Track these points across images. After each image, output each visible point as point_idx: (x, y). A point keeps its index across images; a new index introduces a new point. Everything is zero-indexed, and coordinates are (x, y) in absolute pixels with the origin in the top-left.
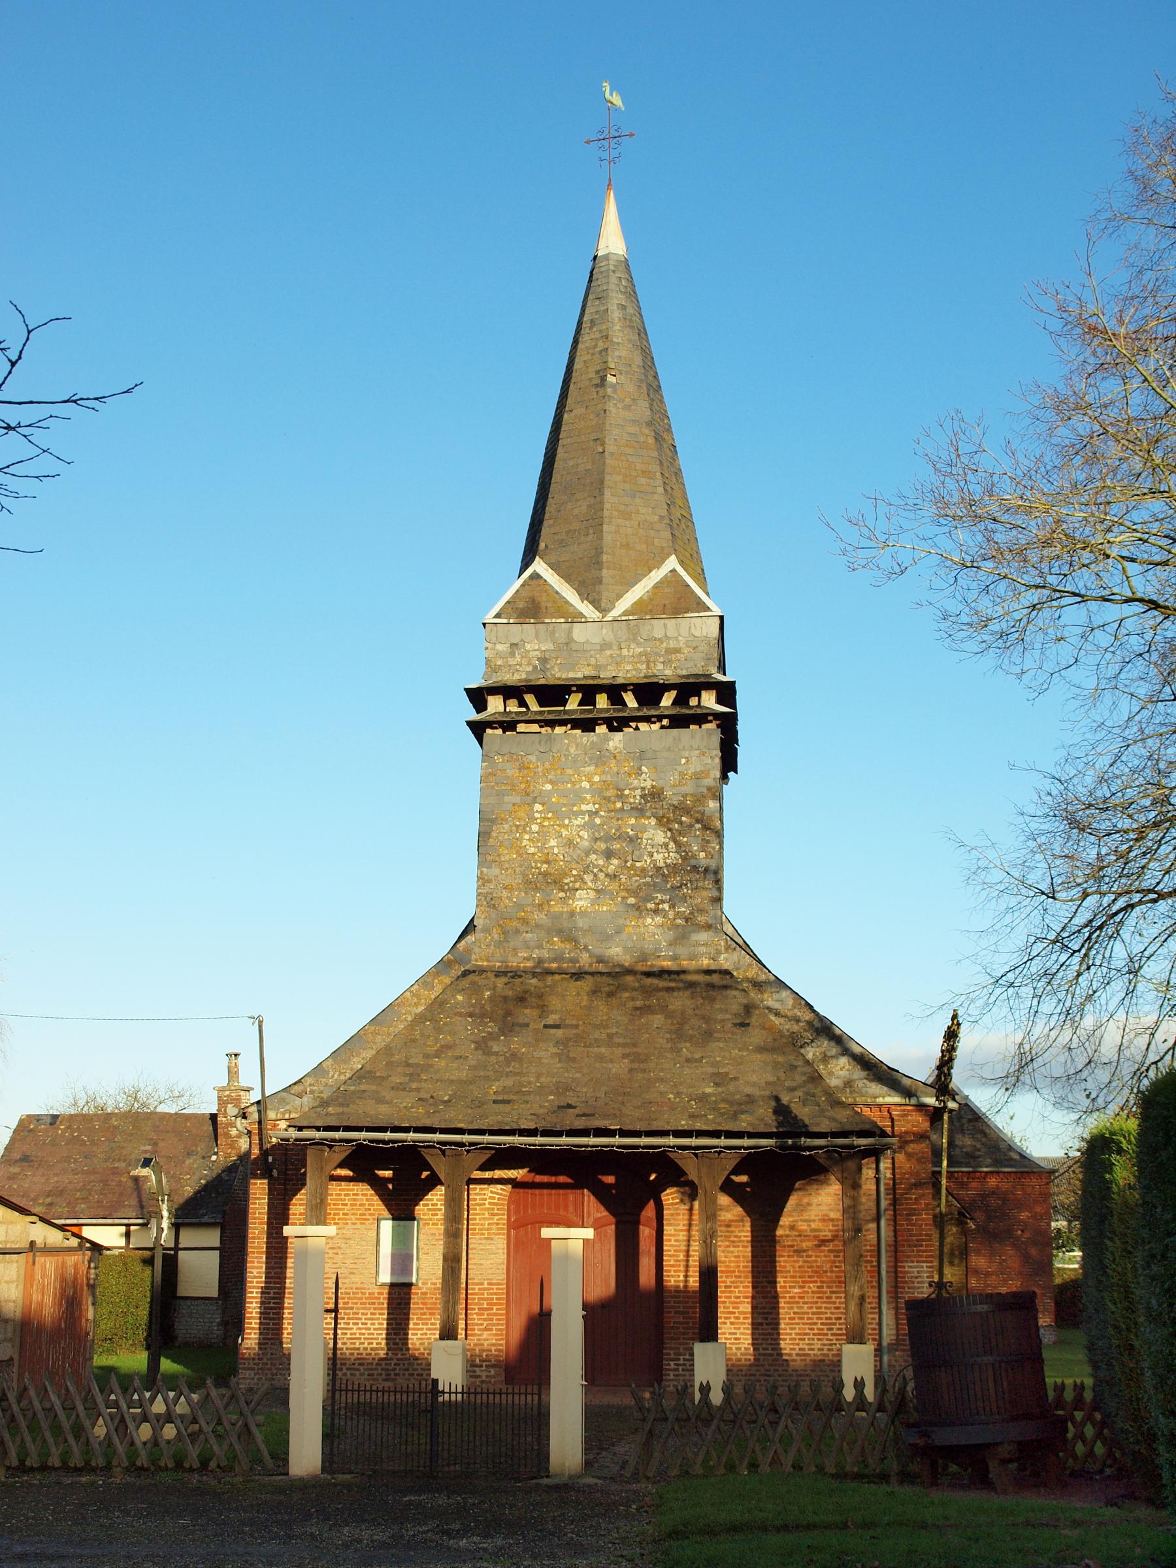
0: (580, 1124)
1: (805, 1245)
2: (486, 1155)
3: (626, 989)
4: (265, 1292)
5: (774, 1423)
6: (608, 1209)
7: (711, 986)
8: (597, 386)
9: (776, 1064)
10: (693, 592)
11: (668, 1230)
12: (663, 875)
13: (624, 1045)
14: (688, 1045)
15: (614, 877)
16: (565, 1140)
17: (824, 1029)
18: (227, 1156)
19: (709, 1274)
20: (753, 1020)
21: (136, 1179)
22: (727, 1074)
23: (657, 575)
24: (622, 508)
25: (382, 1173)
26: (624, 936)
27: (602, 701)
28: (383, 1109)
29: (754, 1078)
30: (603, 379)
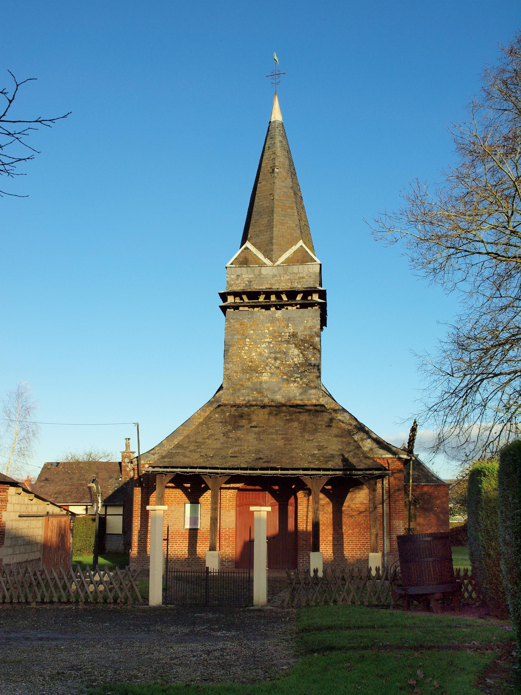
0: (265, 465)
1: (354, 513)
2: (227, 478)
3: (283, 413)
4: (140, 532)
5: (343, 585)
6: (275, 499)
7: (316, 411)
8: (271, 173)
9: (342, 441)
10: (309, 254)
11: (299, 507)
12: (298, 367)
13: (282, 434)
14: (308, 434)
15: (278, 368)
16: (258, 472)
17: (361, 428)
19: (316, 525)
20: (333, 424)
21: (90, 488)
22: (323, 446)
23: (295, 248)
24: (281, 221)
25: (186, 485)
26: (282, 391)
27: (273, 298)
28: (186, 459)
29: (334, 447)
30: (273, 170)
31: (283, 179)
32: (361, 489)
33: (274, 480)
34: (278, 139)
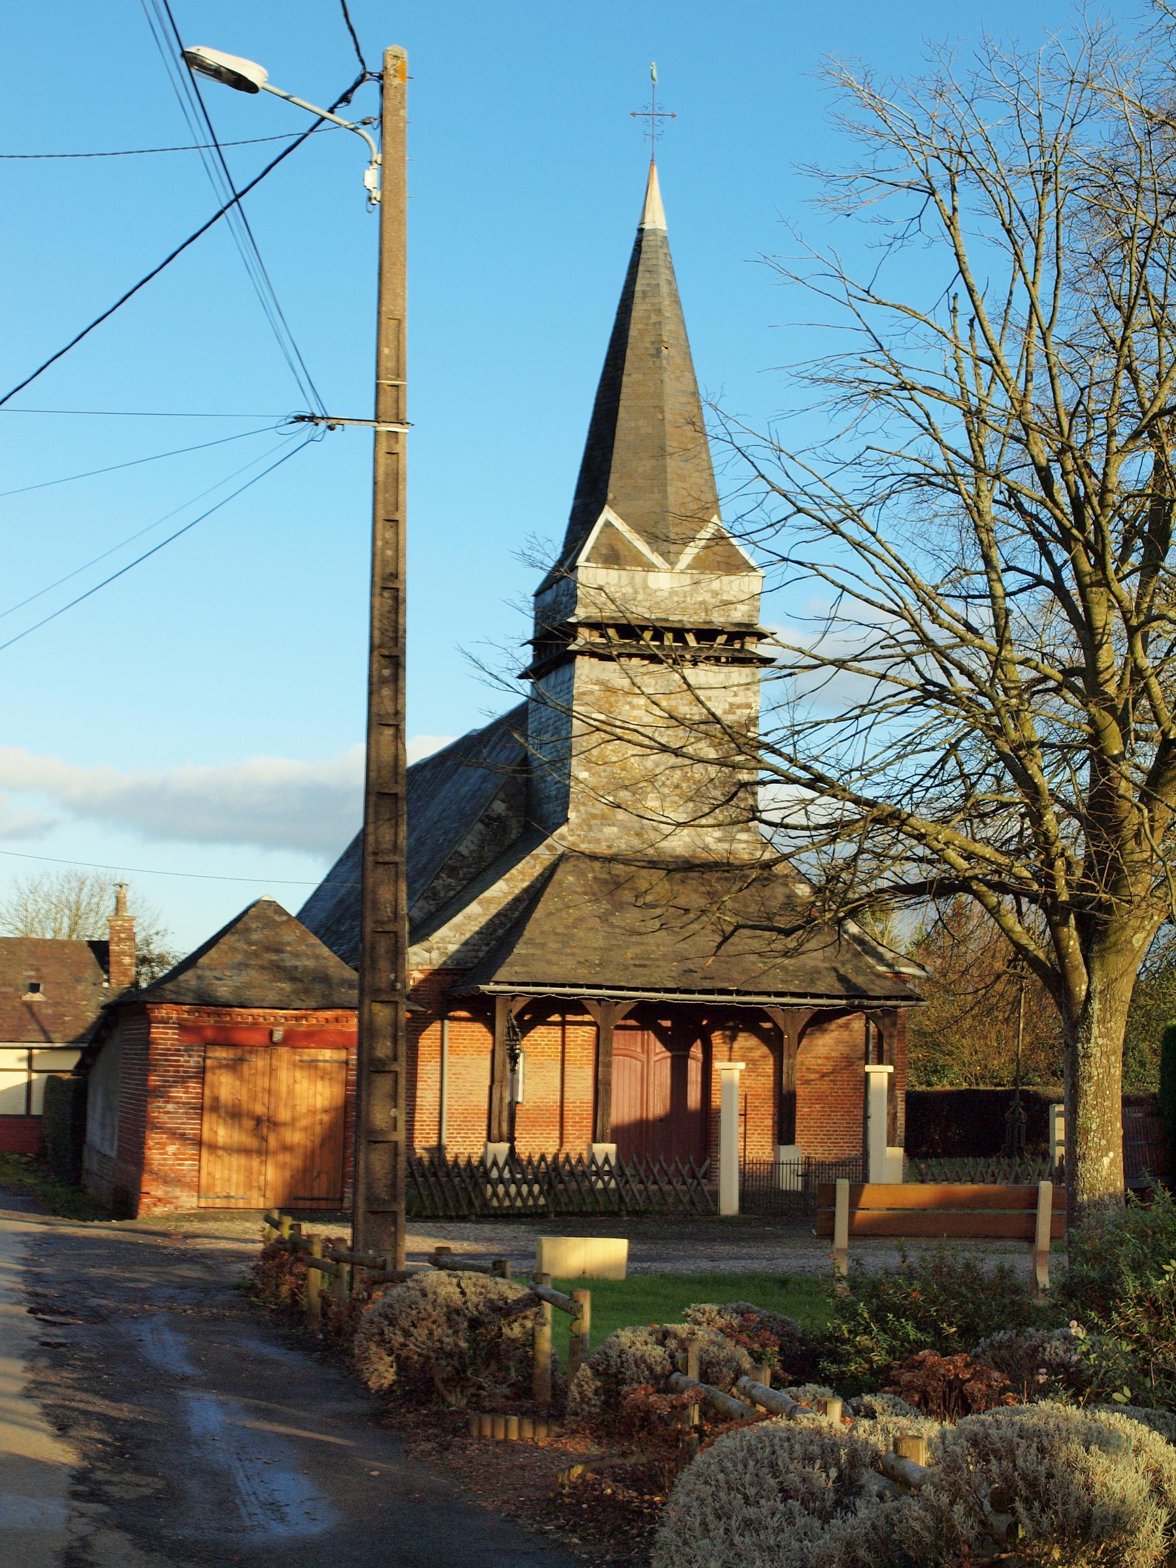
0: (707, 985)
1: (813, 1076)
8: (652, 356)
16: (696, 997)
18: (119, 983)
21: (29, 1006)
24: (679, 471)
27: (669, 638)
28: (555, 969)
30: (659, 351)
31: (678, 373)
32: (825, 1031)
33: (664, 1009)
34: (664, 277)
